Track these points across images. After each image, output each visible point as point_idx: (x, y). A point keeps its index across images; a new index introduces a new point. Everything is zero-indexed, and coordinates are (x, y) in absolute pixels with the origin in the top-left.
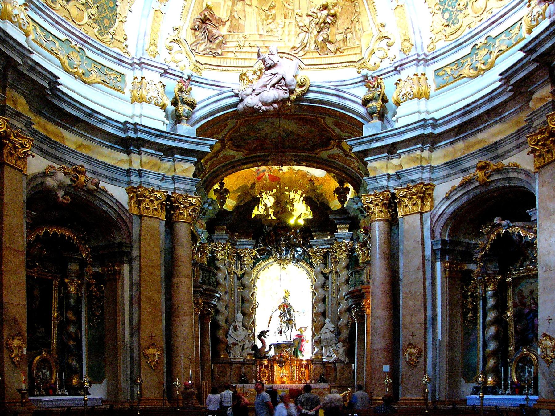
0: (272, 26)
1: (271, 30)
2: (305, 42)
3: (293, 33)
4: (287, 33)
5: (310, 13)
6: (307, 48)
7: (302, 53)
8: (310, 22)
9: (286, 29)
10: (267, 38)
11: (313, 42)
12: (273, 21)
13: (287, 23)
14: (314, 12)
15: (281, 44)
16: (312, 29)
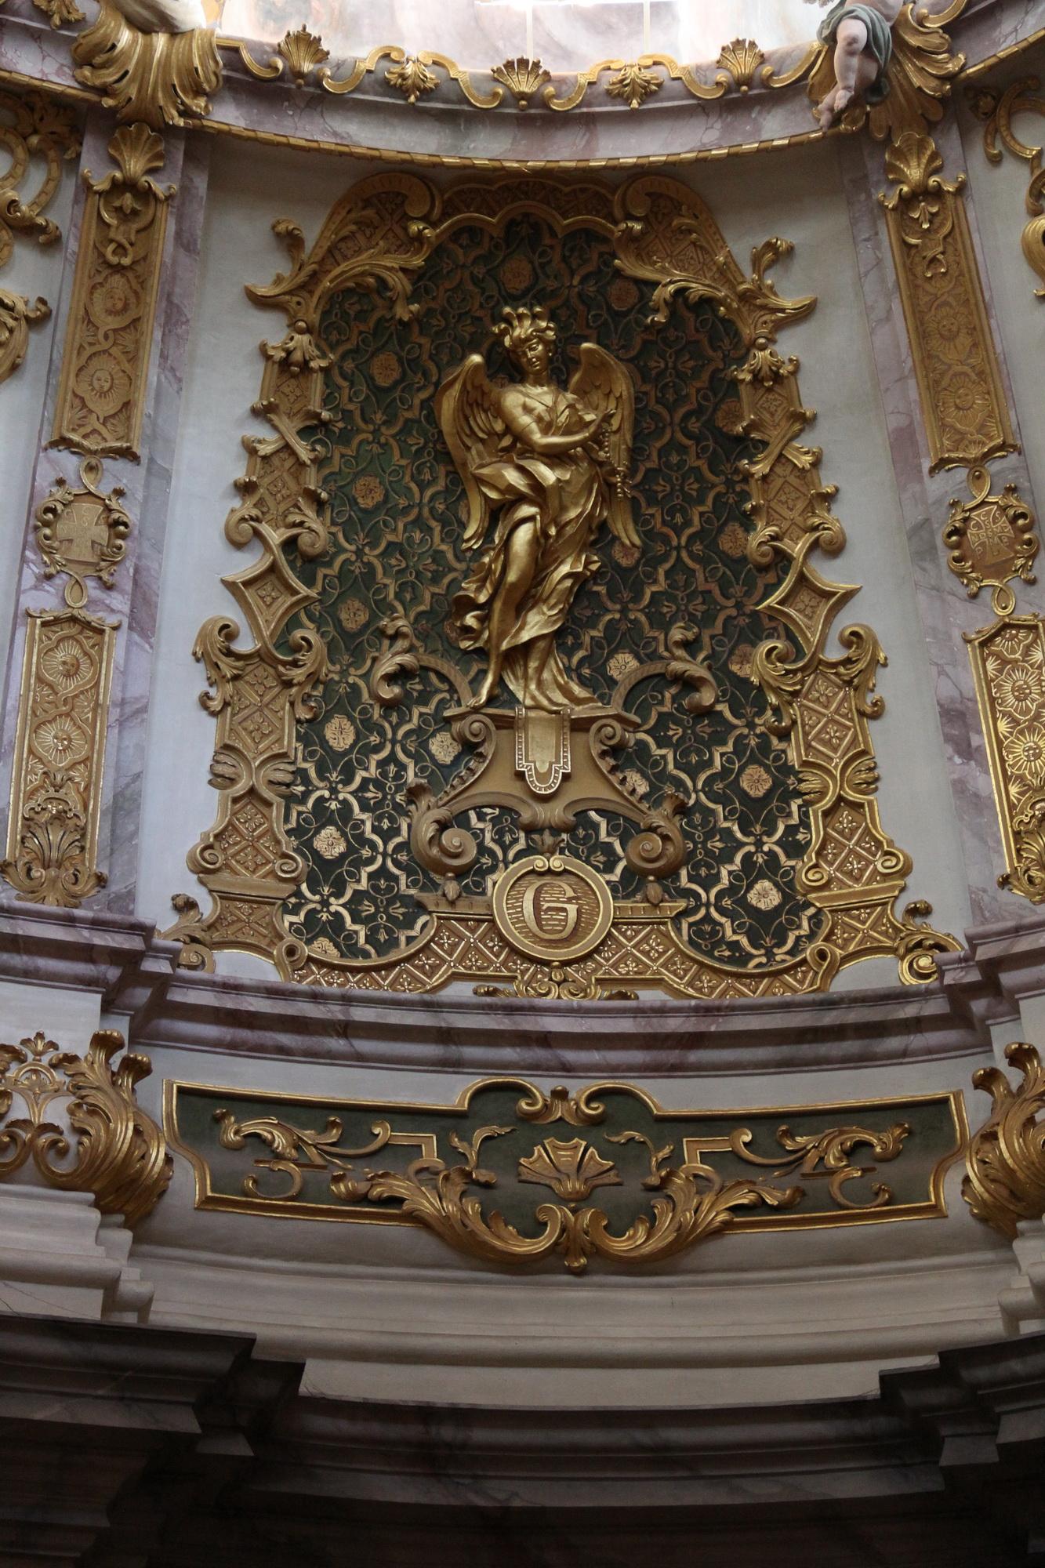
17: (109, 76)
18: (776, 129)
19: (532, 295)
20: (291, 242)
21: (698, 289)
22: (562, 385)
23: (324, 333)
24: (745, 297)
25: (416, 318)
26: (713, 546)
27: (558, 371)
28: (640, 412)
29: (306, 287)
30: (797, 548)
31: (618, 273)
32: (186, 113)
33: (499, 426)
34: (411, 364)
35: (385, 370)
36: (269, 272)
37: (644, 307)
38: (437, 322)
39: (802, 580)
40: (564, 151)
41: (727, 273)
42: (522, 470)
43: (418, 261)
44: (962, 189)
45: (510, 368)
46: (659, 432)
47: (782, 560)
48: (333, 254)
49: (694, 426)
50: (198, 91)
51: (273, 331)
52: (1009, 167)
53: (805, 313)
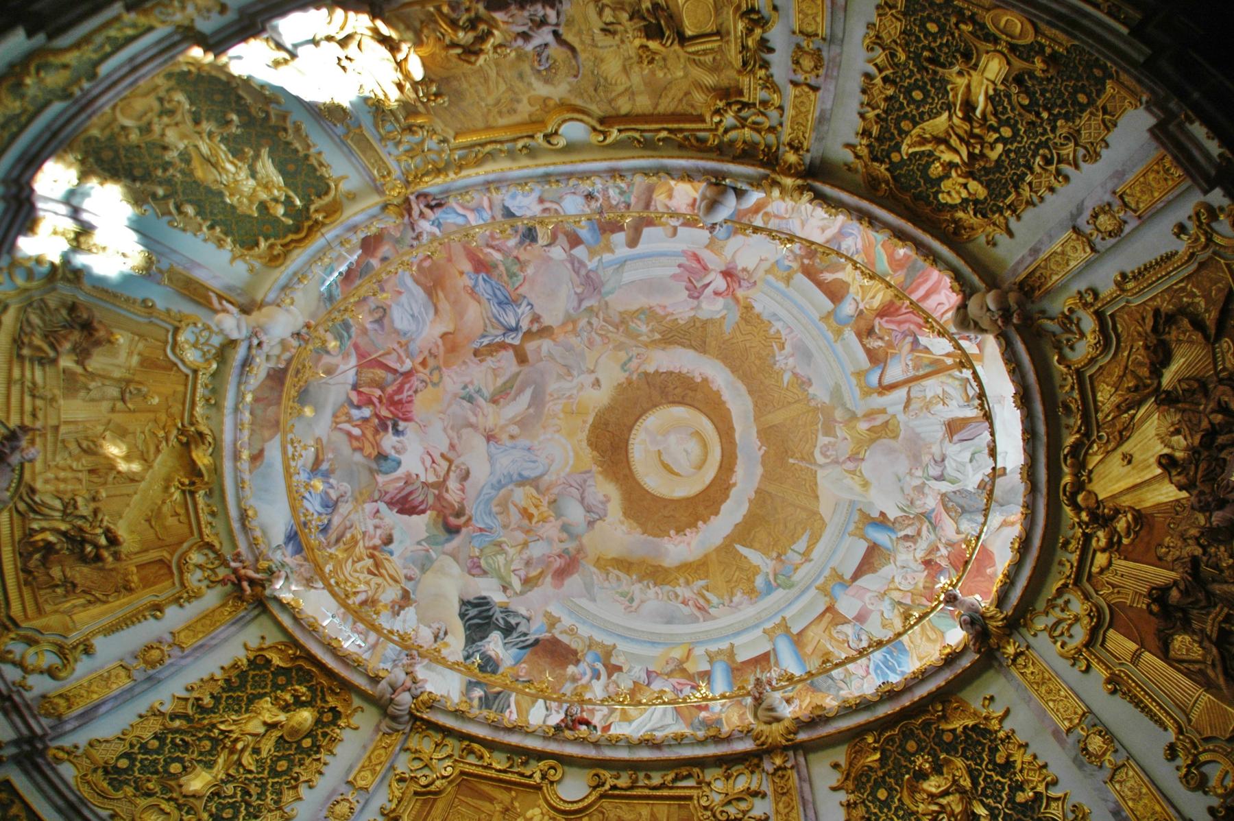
0: (73, 447)
1: (66, 447)
2: (47, 511)
3: (62, 486)
4: (62, 475)
5: (100, 517)
6: (32, 515)
7: (22, 507)
8: (84, 517)
9: (69, 475)
10: (50, 437)
11: (45, 524)
12: (85, 451)
13: (80, 475)
14: (102, 521)
15: (39, 465)
16: (70, 522)
17: (763, 739)
18: (966, 662)
19: (920, 749)
20: (836, 766)
21: (970, 723)
22: (940, 773)
23: (859, 787)
24: (986, 718)
25: (885, 774)
26: (1014, 802)
27: (938, 769)
28: (970, 771)
29: (846, 779)
30: (1041, 788)
31: (943, 731)
32: (788, 740)
33: (925, 796)
34: (890, 790)
35: (882, 794)
36: (835, 778)
37: (956, 737)
38: (893, 772)
39: (1048, 798)
40: (906, 701)
41: (975, 714)
42: (937, 804)
43: (878, 756)
44: (1028, 647)
45: (922, 776)
46: (980, 775)
47: (1038, 796)
48: (851, 764)
49: (990, 767)
50: (790, 733)
51: (842, 796)
52: (1040, 634)
53: (1007, 712)
